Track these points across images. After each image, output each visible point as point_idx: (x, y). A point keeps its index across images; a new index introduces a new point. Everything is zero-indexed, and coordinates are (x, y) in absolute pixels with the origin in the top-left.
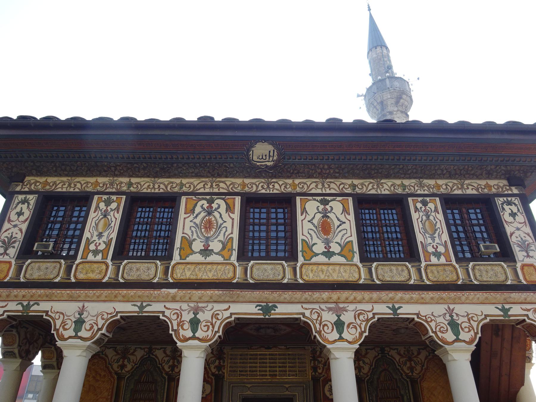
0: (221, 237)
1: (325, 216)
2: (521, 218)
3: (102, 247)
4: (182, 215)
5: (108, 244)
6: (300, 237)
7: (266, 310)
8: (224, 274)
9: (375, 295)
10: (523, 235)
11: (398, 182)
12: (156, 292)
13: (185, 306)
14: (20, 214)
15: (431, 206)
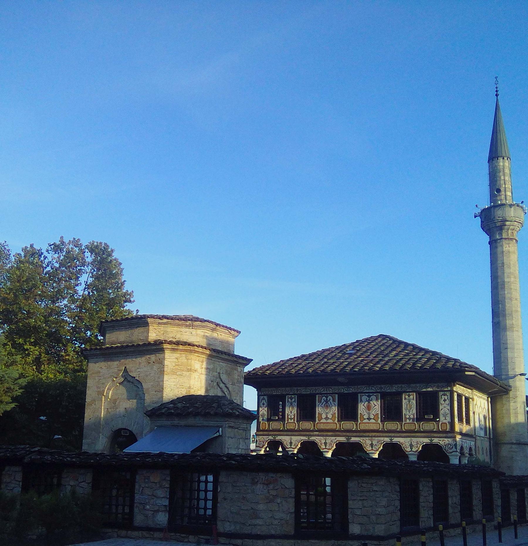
0: (331, 413)
1: (369, 403)
2: (448, 402)
3: (293, 417)
4: (317, 403)
5: (294, 415)
6: (359, 412)
7: (348, 439)
8: (333, 427)
9: (384, 434)
10: (446, 409)
11: (400, 385)
12: (312, 433)
13: (322, 438)
14: (263, 404)
15: (411, 397)
